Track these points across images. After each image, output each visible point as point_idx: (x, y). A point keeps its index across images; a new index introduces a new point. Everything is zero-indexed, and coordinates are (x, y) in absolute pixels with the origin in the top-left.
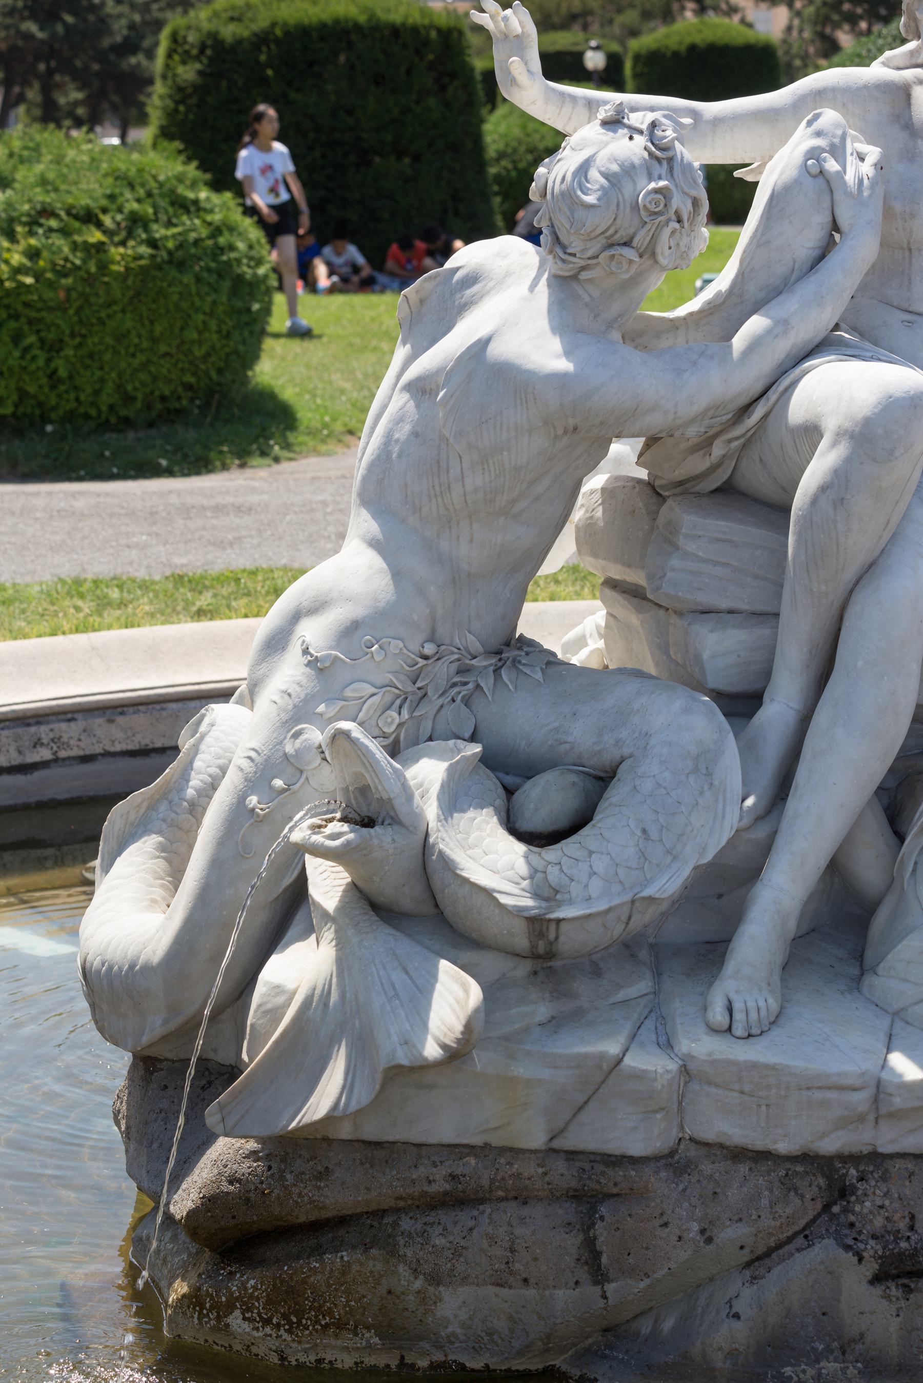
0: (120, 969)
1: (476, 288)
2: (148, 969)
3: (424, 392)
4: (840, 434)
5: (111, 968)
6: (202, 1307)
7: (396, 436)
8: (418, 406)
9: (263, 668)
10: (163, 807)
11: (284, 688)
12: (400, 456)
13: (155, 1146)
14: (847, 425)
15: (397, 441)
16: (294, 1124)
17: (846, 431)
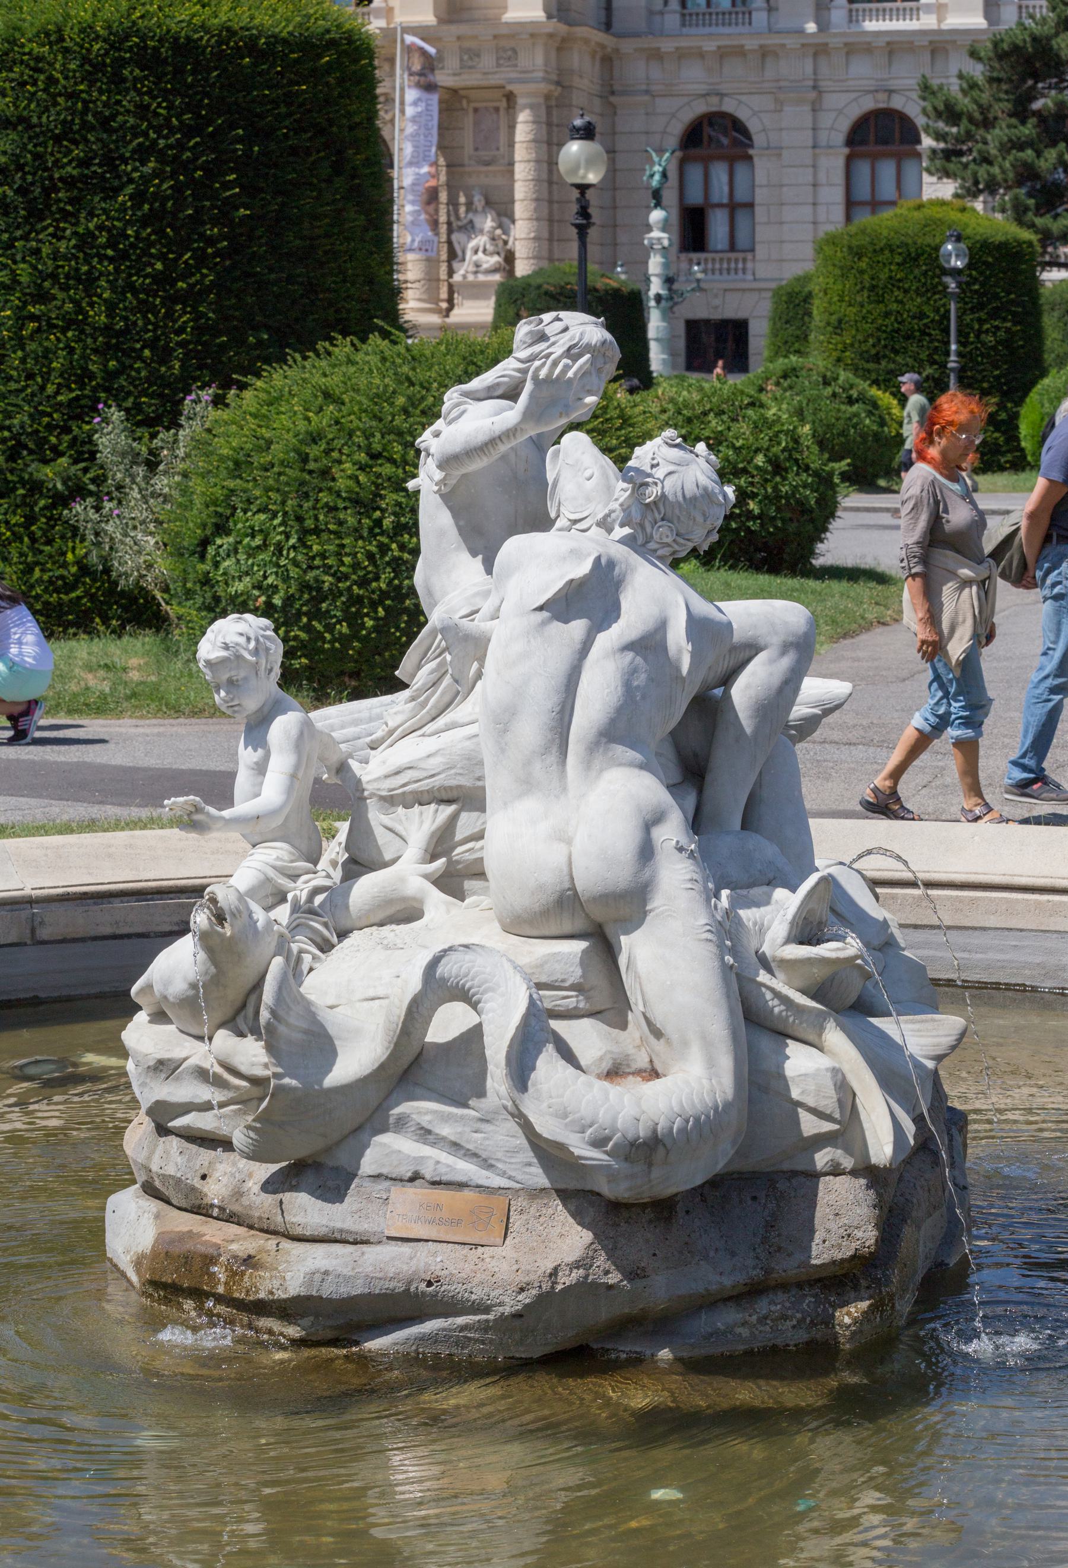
0: (708, 1116)
1: (617, 571)
2: (727, 1105)
3: (646, 648)
4: (785, 648)
5: (697, 1120)
6: (883, 1305)
7: (636, 683)
8: (645, 659)
9: (647, 873)
10: (533, 1022)
11: (688, 877)
12: (643, 697)
13: (712, 1254)
14: (791, 639)
15: (638, 687)
16: (912, 1142)
17: (792, 644)
